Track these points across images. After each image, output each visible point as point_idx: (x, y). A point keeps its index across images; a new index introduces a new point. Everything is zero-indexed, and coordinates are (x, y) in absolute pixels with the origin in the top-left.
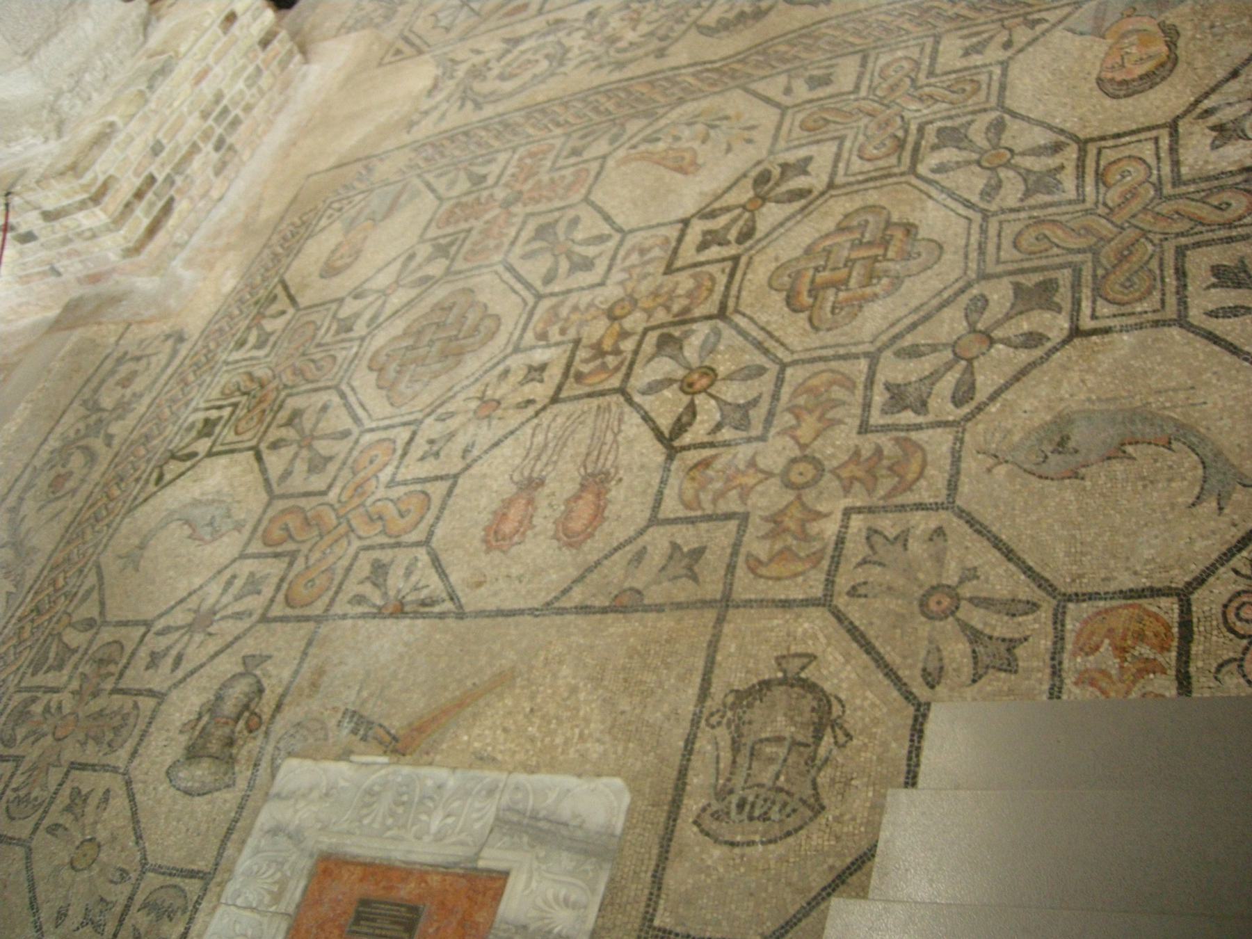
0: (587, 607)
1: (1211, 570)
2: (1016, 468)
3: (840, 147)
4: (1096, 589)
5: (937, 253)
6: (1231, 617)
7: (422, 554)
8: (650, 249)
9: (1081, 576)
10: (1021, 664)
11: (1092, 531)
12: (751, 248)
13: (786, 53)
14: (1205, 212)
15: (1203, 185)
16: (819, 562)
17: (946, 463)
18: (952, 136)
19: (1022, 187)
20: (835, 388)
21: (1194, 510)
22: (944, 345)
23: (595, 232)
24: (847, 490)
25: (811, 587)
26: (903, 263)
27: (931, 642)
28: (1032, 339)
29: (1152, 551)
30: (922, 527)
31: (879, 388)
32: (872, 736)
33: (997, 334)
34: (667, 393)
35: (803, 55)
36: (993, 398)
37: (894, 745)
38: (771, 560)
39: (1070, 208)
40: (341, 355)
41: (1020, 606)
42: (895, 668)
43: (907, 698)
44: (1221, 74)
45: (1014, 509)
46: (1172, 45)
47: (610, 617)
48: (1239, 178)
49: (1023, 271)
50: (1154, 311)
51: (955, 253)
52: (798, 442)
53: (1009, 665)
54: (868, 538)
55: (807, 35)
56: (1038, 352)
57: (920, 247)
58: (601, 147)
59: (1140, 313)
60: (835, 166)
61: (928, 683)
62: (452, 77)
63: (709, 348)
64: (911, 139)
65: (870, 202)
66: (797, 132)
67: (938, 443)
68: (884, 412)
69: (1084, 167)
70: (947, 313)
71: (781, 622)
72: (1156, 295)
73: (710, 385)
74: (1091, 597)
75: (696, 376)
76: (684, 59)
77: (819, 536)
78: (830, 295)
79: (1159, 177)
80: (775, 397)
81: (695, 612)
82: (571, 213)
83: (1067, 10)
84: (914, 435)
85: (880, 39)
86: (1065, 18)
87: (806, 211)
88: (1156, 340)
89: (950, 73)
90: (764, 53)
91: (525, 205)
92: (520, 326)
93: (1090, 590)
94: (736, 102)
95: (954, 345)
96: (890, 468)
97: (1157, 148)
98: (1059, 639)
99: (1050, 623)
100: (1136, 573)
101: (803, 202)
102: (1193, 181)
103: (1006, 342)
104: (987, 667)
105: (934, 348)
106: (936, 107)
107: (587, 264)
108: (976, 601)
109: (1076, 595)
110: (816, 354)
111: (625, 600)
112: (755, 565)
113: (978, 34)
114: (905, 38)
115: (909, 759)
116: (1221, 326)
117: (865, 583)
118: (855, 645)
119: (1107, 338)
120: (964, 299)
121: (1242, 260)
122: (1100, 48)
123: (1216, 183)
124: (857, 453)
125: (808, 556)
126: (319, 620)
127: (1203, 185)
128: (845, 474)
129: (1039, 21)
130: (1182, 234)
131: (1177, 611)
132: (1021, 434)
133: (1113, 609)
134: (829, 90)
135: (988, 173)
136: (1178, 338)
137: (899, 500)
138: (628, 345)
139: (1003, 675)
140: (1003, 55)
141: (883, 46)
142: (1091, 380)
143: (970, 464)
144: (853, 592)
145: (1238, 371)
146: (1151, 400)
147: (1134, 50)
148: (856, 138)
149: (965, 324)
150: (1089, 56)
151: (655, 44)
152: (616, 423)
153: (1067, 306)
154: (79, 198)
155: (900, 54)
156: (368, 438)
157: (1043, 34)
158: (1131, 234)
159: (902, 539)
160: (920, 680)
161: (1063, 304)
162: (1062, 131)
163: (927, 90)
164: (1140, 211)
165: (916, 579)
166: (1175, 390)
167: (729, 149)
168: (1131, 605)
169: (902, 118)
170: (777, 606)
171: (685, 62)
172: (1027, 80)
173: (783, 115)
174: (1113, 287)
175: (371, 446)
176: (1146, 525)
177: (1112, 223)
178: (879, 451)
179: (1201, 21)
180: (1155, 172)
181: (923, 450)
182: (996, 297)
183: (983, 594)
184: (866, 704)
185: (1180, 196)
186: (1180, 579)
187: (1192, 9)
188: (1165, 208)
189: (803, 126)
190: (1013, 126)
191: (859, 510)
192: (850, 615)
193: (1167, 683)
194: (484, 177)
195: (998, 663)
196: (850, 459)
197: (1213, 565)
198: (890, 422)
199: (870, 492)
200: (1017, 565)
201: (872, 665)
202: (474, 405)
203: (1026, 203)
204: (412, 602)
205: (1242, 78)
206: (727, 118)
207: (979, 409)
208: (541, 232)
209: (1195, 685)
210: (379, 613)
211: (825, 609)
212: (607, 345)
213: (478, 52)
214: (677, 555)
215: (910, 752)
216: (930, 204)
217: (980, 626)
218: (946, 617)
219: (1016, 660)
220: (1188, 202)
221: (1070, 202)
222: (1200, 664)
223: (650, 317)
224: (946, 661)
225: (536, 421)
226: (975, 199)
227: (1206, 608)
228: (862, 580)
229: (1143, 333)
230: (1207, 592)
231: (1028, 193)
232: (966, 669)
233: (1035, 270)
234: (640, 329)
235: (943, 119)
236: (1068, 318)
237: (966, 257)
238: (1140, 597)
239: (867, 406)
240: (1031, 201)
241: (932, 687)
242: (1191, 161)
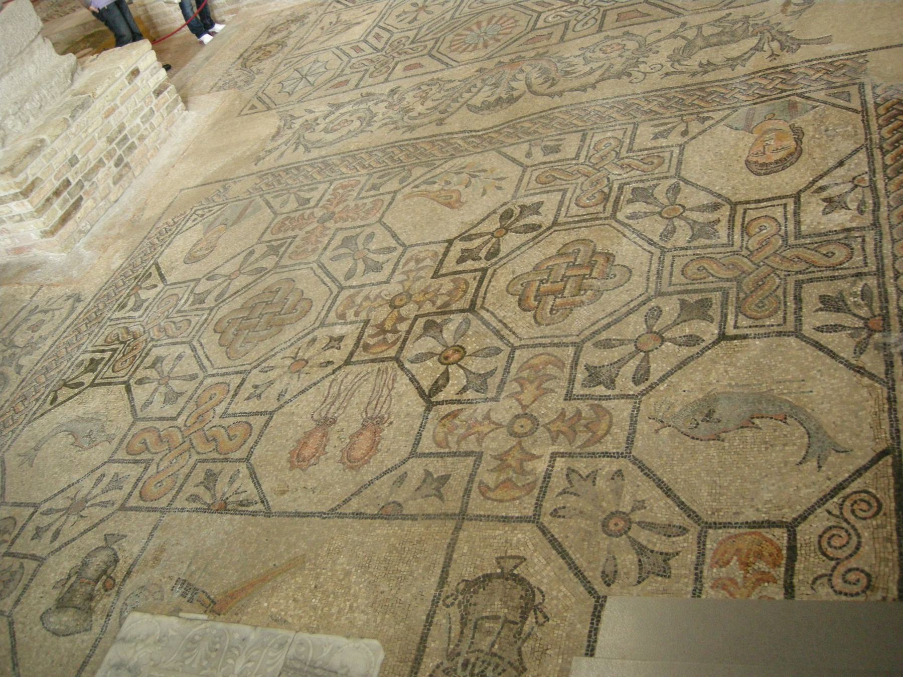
0: (361, 513)
1: (811, 510)
2: (676, 431)
3: (563, 196)
4: (729, 520)
5: (627, 275)
6: (824, 544)
7: (243, 467)
8: (423, 260)
9: (718, 510)
10: (673, 571)
11: (728, 478)
12: (496, 263)
13: (529, 128)
14: (817, 258)
15: (816, 239)
16: (531, 491)
17: (627, 425)
18: (643, 194)
19: (690, 233)
20: (550, 366)
21: (800, 467)
23: (385, 245)
24: (554, 440)
25: (525, 508)
26: (603, 281)
27: (609, 553)
28: (692, 340)
29: (770, 495)
30: (607, 469)
31: (581, 368)
32: (564, 619)
33: (667, 335)
34: (429, 363)
35: (540, 130)
36: (662, 380)
37: (579, 626)
38: (497, 487)
39: (723, 250)
40: (194, 320)
41: (674, 529)
42: (582, 569)
43: (590, 592)
44: (832, 163)
45: (673, 460)
46: (799, 141)
47: (377, 522)
48: (841, 236)
49: (687, 292)
50: (778, 325)
51: (640, 276)
52: (521, 404)
53: (664, 571)
54: (567, 475)
55: (545, 116)
56: (695, 350)
57: (616, 270)
58: (394, 185)
59: (769, 326)
60: (559, 209)
61: (605, 582)
62: (291, 128)
63: (461, 333)
64: (614, 195)
66: (533, 184)
67: (621, 410)
68: (584, 385)
69: (733, 221)
70: (632, 318)
71: (501, 532)
72: (780, 314)
73: (460, 360)
74: (726, 525)
75: (450, 352)
76: (457, 127)
77: (532, 472)
78: (550, 299)
79: (786, 232)
80: (507, 370)
81: (440, 521)
82: (368, 230)
84: (604, 403)
85: (596, 123)
86: (726, 117)
87: (537, 240)
88: (778, 345)
89: (644, 150)
90: (514, 127)
91: (336, 222)
92: (326, 308)
93: (724, 521)
94: (491, 160)
96: (586, 426)
97: (785, 212)
98: (701, 554)
99: (695, 542)
100: (758, 510)
102: (809, 236)
103: (673, 341)
104: (649, 573)
105: (622, 342)
106: (632, 173)
107: (378, 268)
108: (642, 525)
109: (715, 523)
110: (537, 341)
111: (389, 509)
112: (484, 490)
113: (666, 124)
114: (613, 124)
115: (590, 636)
116: (825, 338)
117: (564, 508)
118: (554, 552)
119: (745, 342)
120: (645, 309)
121: (841, 293)
122: (750, 139)
123: (825, 238)
124: (563, 414)
125: (524, 486)
126: (163, 511)
127: (816, 239)
128: (554, 428)
129: (708, 118)
130: (800, 272)
131: (786, 538)
132: (681, 407)
133: (740, 535)
134: (557, 156)
135: (667, 221)
136: (794, 344)
137: (591, 449)
138: (403, 327)
139: (660, 579)
140: (681, 140)
141: (597, 128)
142: (732, 371)
143: (643, 426)
144: (555, 513)
145: (835, 370)
146: (773, 387)
147: (772, 142)
148: (574, 191)
149: (645, 326)
150: (741, 145)
151: (436, 116)
152: (391, 382)
153: (717, 318)
154: (12, 191)
155: (609, 134)
156: (209, 381)
158: (764, 270)
159: (592, 477)
160: (600, 579)
161: (714, 317)
162: (720, 196)
163: (626, 161)
164: (771, 255)
165: (601, 506)
166: (791, 381)
167: (484, 194)
168: (753, 533)
169: (608, 179)
170: (499, 521)
171: (457, 130)
172: (697, 158)
173: (524, 172)
174: (750, 306)
175: (211, 387)
176: (766, 476)
177: (752, 261)
178: (578, 413)
179: (819, 126)
180: (783, 228)
181: (610, 414)
182: (667, 308)
183: (648, 520)
184: (560, 595)
185: (800, 246)
186: (789, 515)
187: (814, 117)
188: (788, 253)
189: (537, 180)
190: (686, 190)
191: (562, 455)
192: (552, 530)
193: (777, 590)
194: (308, 200)
195: (656, 570)
197: (813, 506)
198: (588, 393)
200: (673, 500)
201: (566, 567)
202: (288, 362)
203: (692, 244)
204: (233, 502)
205: (846, 167)
206: (485, 171)
207: (652, 387)
208: (346, 242)
209: (797, 592)
210: (208, 509)
212: (388, 326)
213: (311, 112)
214: (429, 480)
215: (590, 632)
216: (625, 240)
217: (644, 543)
218: (621, 535)
219: (670, 568)
220: (805, 250)
221: (723, 245)
222: (801, 577)
223: (420, 308)
224: (619, 567)
225: (333, 377)
226: (656, 239)
227: (807, 537)
228: (562, 505)
229: (770, 340)
230: (808, 526)
231: (693, 238)
232: (633, 573)
233: (696, 291)
234: (412, 316)
235: (637, 182)
236: (717, 326)
237: (648, 280)
238: (760, 527)
239: (572, 381)
240: (695, 243)
241: (609, 585)
242: (808, 221)
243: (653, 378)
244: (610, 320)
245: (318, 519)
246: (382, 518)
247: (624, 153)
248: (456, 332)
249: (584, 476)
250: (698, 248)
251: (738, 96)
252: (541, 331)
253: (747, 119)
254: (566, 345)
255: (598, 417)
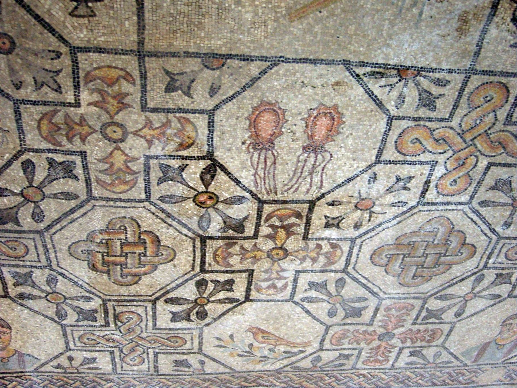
0: (244, 60)
7: (394, 111)
8: (269, 287)
13: (211, 384)
22: (50, 197)
25: (86, 60)
26: (90, 249)
30: (29, 91)
38: (118, 79)
40: (502, 258)
42: (18, 5)
47: (224, 51)
51: (61, 249)
65: (124, 288)
66: (188, 338)
71: (99, 39)
77: (92, 91)
81: (160, 50)
82: (335, 320)
83: (43, 369)
91: (374, 331)
92: (354, 255)
95: (44, 197)
96: (59, 129)
101: (169, 296)
106: (102, 334)
107: (312, 285)
111: (216, 63)
112: (128, 77)
118: (47, 21)
124: (83, 140)
125: (95, 79)
126: (476, 72)
134: (175, 357)
137: (48, 109)
144: (59, 55)
152: (259, 181)
156: (464, 198)
157: (51, 360)
159: (39, 85)
165: (21, 59)
167: (231, 336)
170: (105, 49)
175: (459, 193)
181: (42, 137)
191: (70, 105)
192: (56, 40)
194: (412, 354)
196: (86, 137)
198: (68, 156)
199: (67, 116)
201: (32, 7)
202: (376, 209)
204: (391, 76)
208: (358, 313)
210: (419, 71)
211: (73, 45)
212: (282, 233)
214: (185, 89)
216: (87, 281)
223: (255, 245)
225: (323, 191)
226: (60, 278)
231: (30, 274)
239: (85, 168)
243: (17, 165)
244: (72, 216)
245: (288, 56)
246: (220, 55)
247: (116, 350)
248: (210, 221)
249: (45, 86)
250: (23, 266)
251: (38, 381)
252: (128, 213)
253: (23, 362)
254: (101, 198)
255: (52, 135)
